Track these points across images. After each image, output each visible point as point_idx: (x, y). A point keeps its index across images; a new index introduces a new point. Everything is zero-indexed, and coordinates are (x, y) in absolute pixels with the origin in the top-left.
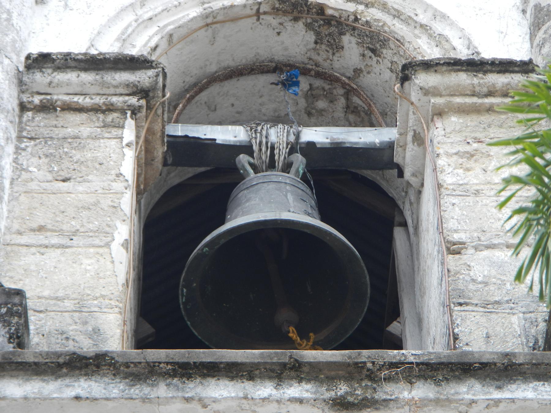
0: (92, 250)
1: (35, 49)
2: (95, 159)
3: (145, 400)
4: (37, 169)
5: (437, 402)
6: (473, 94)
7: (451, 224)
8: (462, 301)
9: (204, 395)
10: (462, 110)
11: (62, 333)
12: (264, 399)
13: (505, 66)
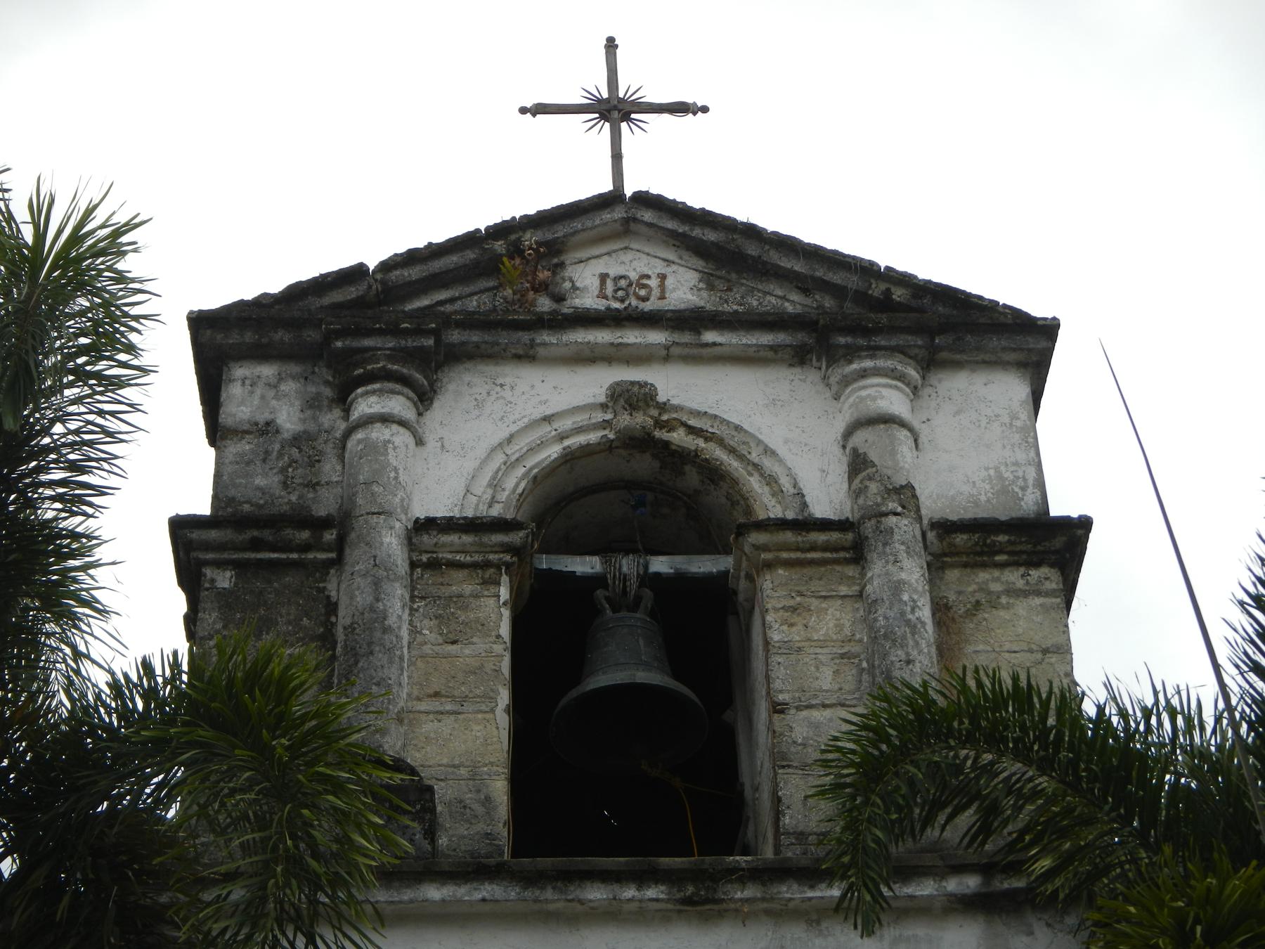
0: (480, 716)
2: (477, 620)
3: (536, 901)
5: (763, 899)
6: (798, 549)
7: (777, 684)
8: (785, 763)
9: (581, 897)
10: (788, 564)
11: (461, 802)
12: (629, 900)
13: (825, 525)
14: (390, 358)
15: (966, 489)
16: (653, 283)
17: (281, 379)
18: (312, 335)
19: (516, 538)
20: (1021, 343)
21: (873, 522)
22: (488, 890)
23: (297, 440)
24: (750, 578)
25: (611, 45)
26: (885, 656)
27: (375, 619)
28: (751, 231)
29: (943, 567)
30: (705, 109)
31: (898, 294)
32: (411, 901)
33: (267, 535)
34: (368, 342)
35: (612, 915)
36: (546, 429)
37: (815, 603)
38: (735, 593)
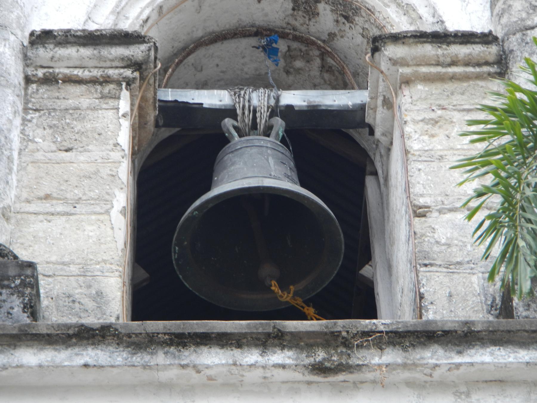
0: (93, 217)
1: (38, 26)
2: (94, 130)
3: (145, 367)
4: (42, 140)
5: (405, 366)
6: (438, 64)
7: (417, 189)
8: (427, 262)
9: (198, 362)
10: (428, 79)
11: (69, 297)
12: (251, 366)
13: (467, 38)
21: (518, 35)
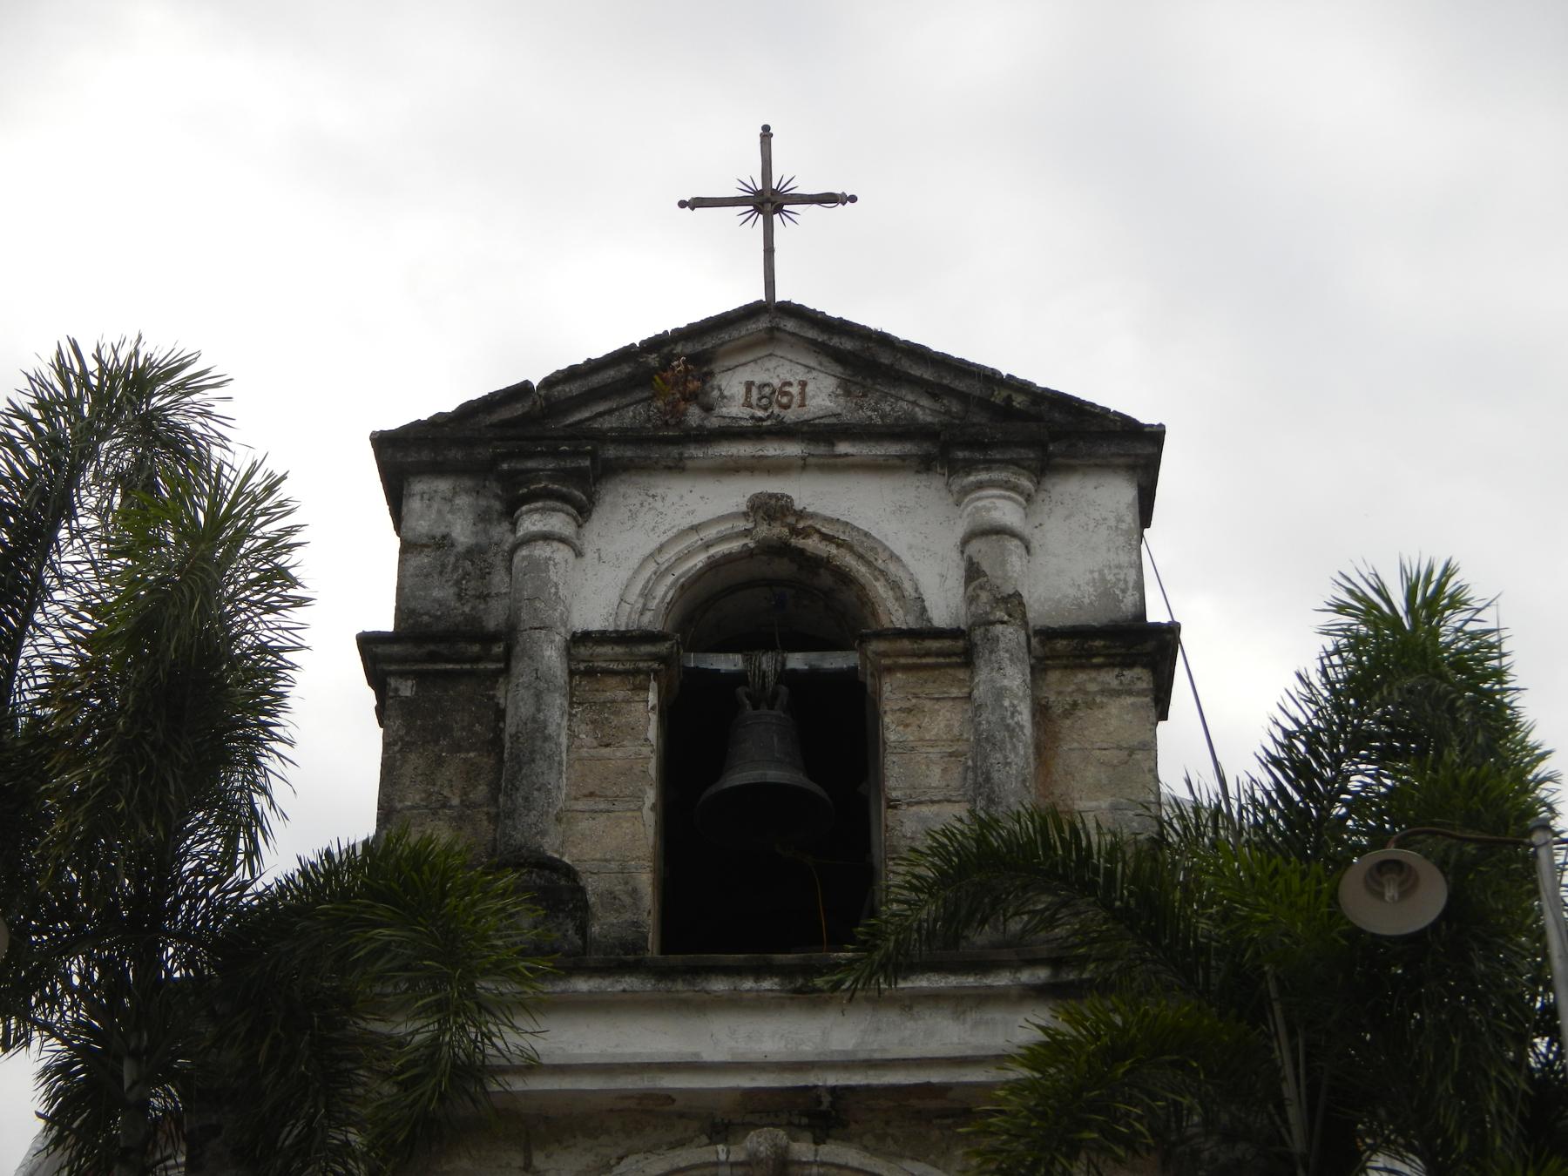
10: (907, 668)
13: (939, 634)
14: (552, 478)
15: (1072, 592)
16: (795, 390)
17: (455, 493)
18: (483, 453)
19: (663, 648)
20: (1132, 449)
21: (982, 629)
22: (628, 983)
23: (471, 553)
24: (872, 675)
25: (766, 133)
26: (986, 758)
27: (537, 729)
28: (884, 340)
29: (1045, 670)
30: (853, 199)
31: (1019, 401)
32: (563, 992)
33: (443, 648)
34: (531, 464)
35: (734, 1003)
36: (694, 539)
37: (928, 704)
38: (863, 685)
